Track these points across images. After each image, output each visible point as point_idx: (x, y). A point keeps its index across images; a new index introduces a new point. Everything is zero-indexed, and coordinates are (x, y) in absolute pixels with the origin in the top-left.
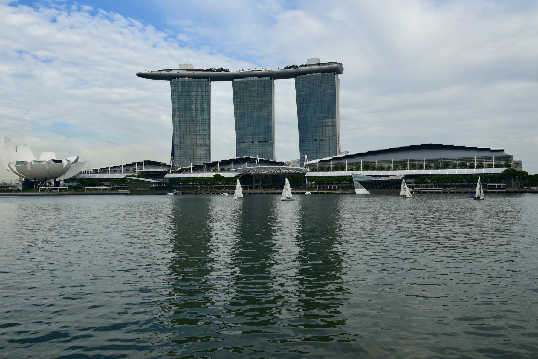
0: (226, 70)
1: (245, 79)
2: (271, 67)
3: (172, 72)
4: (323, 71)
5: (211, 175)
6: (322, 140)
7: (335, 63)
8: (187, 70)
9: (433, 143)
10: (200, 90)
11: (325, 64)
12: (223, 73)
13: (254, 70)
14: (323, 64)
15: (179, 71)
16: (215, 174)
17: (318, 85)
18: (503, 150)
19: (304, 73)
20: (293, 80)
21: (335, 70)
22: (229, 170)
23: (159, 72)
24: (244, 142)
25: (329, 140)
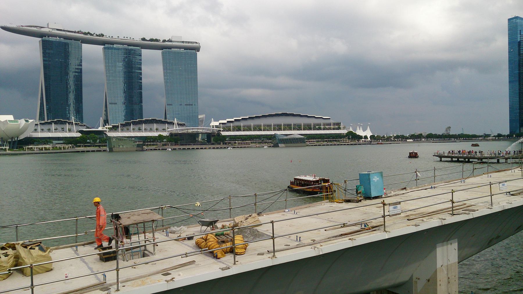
1: (115, 46)
3: (42, 30)
4: (186, 48)
5: (156, 134)
6: (186, 105)
7: (197, 43)
11: (189, 42)
12: (89, 36)
15: (51, 30)
19: (170, 48)
20: (159, 52)
21: (198, 49)
22: (151, 130)
23: (25, 28)
24: (116, 104)
25: (192, 105)
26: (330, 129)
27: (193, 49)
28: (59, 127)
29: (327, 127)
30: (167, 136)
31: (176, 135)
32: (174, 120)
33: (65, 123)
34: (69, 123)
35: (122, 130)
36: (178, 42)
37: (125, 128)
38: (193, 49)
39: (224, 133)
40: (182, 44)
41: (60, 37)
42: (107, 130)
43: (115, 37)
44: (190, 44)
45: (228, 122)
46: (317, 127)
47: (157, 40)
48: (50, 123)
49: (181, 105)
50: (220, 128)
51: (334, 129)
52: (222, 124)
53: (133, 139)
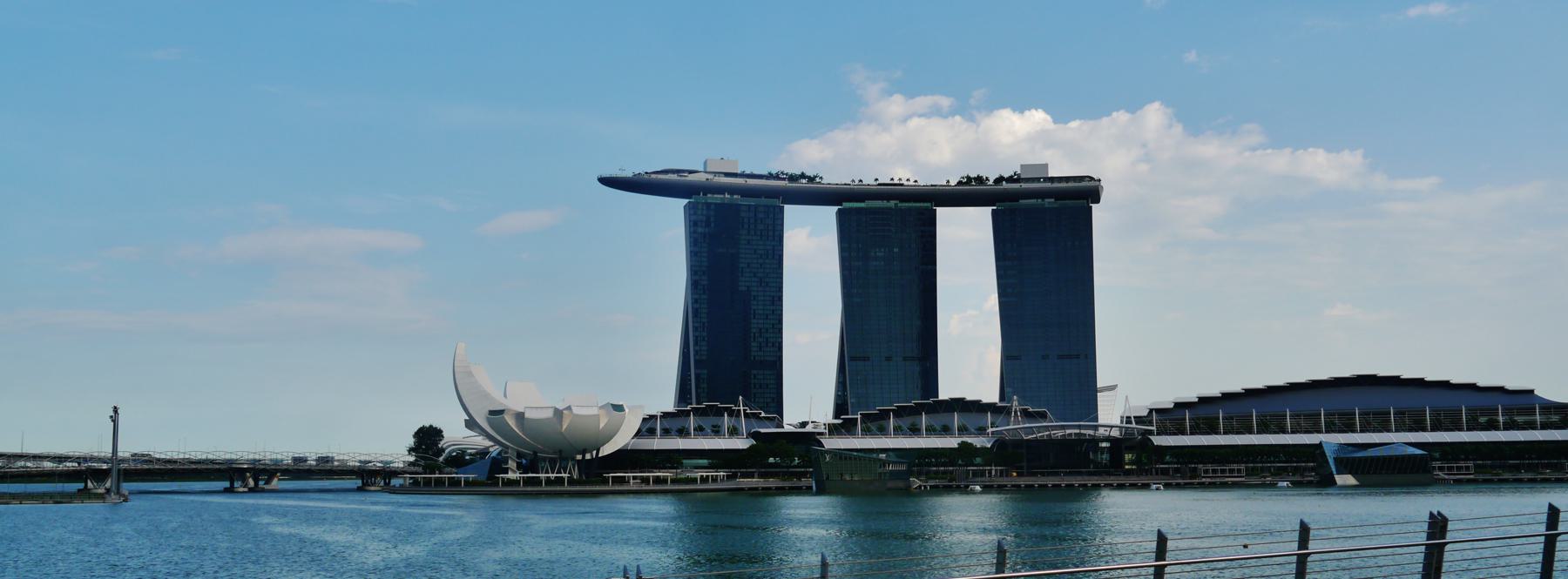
0: (811, 179)
2: (926, 179)
3: (691, 177)
4: (1059, 195)
5: (951, 442)
6: (1061, 357)
7: (1091, 179)
9: (1381, 374)
10: (761, 227)
11: (1067, 179)
14: (1060, 179)
16: (960, 440)
17: (1046, 229)
18: (1532, 391)
24: (866, 359)
25: (1078, 357)
26: (1531, 426)
27: (1079, 197)
28: (707, 422)
29: (1520, 419)
31: (1019, 444)
33: (719, 412)
35: (867, 432)
36: (1037, 180)
38: (1079, 197)
39: (1158, 440)
40: (1048, 185)
41: (732, 190)
43: (869, 180)
44: (1071, 184)
46: (1483, 420)
47: (979, 180)
49: (1044, 357)
50: (1151, 423)
51: (1544, 427)
52: (1159, 411)
53: (883, 456)
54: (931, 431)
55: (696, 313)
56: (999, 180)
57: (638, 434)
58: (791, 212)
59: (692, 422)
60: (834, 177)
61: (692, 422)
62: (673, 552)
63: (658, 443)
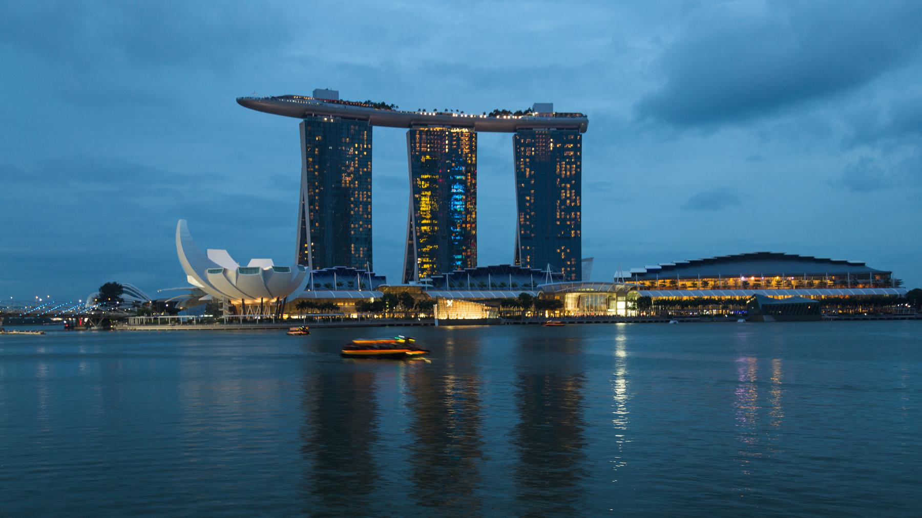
5: (514, 294)
7: (581, 115)
8: (333, 102)
13: (443, 111)
16: (521, 292)
17: (551, 149)
22: (503, 287)
27: (571, 129)
30: (536, 298)
32: (545, 268)
33: (354, 274)
34: (362, 274)
37: (457, 283)
38: (571, 129)
42: (427, 285)
45: (648, 270)
48: (330, 274)
54: (494, 287)
55: (312, 202)
56: (519, 113)
57: (308, 287)
58: (375, 129)
59: (335, 279)
60: (405, 105)
61: (335, 279)
62: (590, 351)
63: (316, 294)
